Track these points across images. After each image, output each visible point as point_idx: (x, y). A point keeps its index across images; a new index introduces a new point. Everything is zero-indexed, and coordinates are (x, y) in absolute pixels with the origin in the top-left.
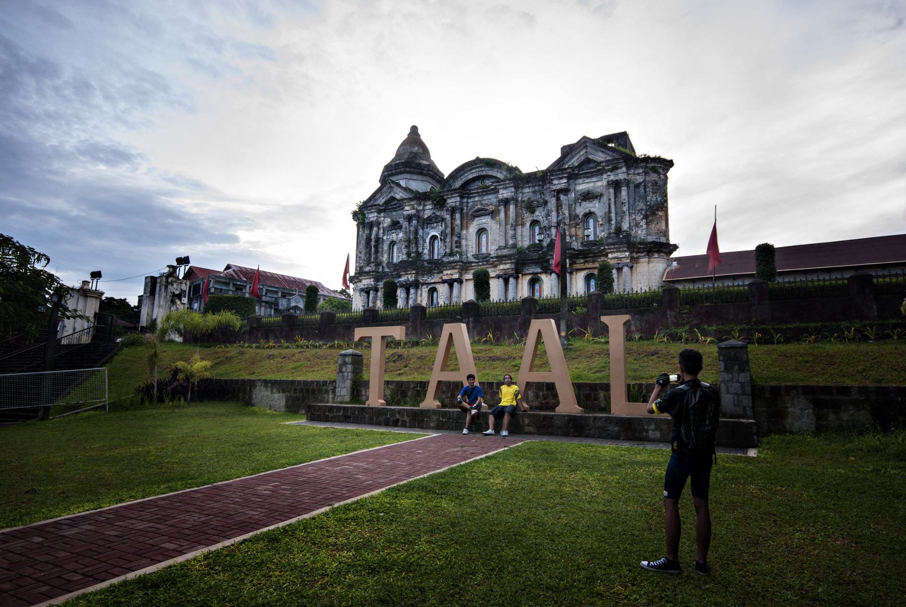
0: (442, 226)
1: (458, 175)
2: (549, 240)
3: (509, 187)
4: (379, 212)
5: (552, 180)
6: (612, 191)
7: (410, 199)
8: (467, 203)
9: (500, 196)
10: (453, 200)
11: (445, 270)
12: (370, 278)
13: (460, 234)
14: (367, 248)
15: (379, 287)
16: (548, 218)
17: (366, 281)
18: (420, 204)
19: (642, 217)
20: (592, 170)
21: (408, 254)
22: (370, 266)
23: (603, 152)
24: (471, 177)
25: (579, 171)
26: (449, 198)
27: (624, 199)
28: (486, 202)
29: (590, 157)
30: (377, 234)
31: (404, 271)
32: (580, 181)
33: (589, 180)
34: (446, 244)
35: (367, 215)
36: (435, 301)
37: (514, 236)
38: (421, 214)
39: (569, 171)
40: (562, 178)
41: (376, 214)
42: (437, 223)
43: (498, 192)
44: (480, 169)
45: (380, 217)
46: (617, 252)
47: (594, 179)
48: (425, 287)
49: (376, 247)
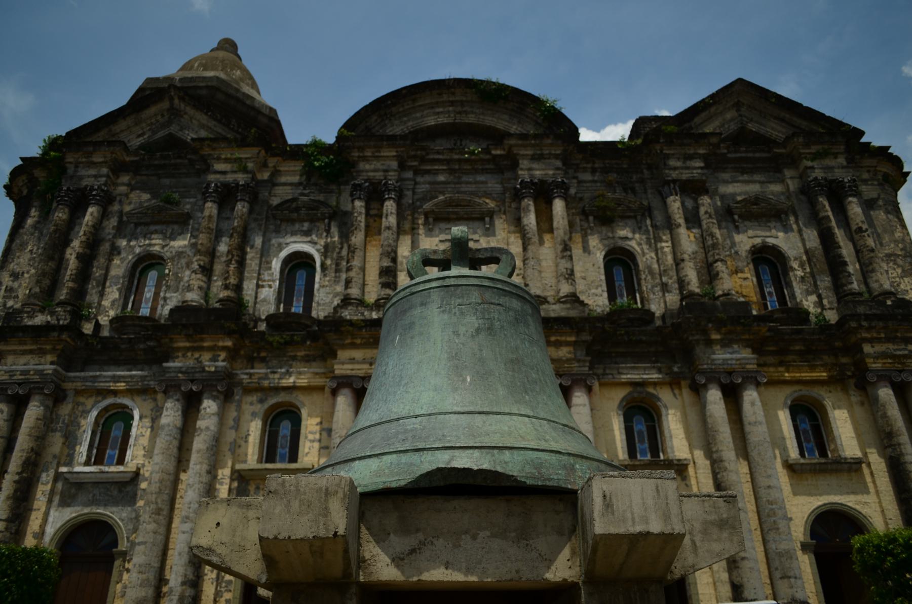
0: (328, 231)
1: (394, 109)
2: (673, 299)
3: (551, 156)
4: (118, 168)
5: (668, 157)
6: (823, 201)
7: (243, 143)
8: (416, 183)
9: (524, 175)
10: (378, 165)
11: (344, 347)
12: (42, 352)
13: (396, 252)
14: (51, 258)
15: (69, 386)
16: (659, 245)
17: (23, 359)
18: (265, 165)
19: (899, 271)
20: (758, 155)
21: (206, 293)
22: (52, 313)
23: (783, 120)
24: (431, 121)
25: (729, 152)
26: (365, 159)
27: (863, 222)
28: (472, 188)
29: (750, 126)
30: (97, 227)
31: (188, 337)
32: (726, 176)
33: (746, 177)
34: (352, 274)
35: (70, 171)
36: (283, 449)
37: (570, 275)
38: (264, 194)
39: (714, 140)
40: (691, 157)
41: (105, 170)
42: (312, 221)
43: (514, 166)
44: (459, 109)
45: (116, 185)
46: (888, 340)
47: (757, 177)
48: (254, 398)
49: (86, 260)
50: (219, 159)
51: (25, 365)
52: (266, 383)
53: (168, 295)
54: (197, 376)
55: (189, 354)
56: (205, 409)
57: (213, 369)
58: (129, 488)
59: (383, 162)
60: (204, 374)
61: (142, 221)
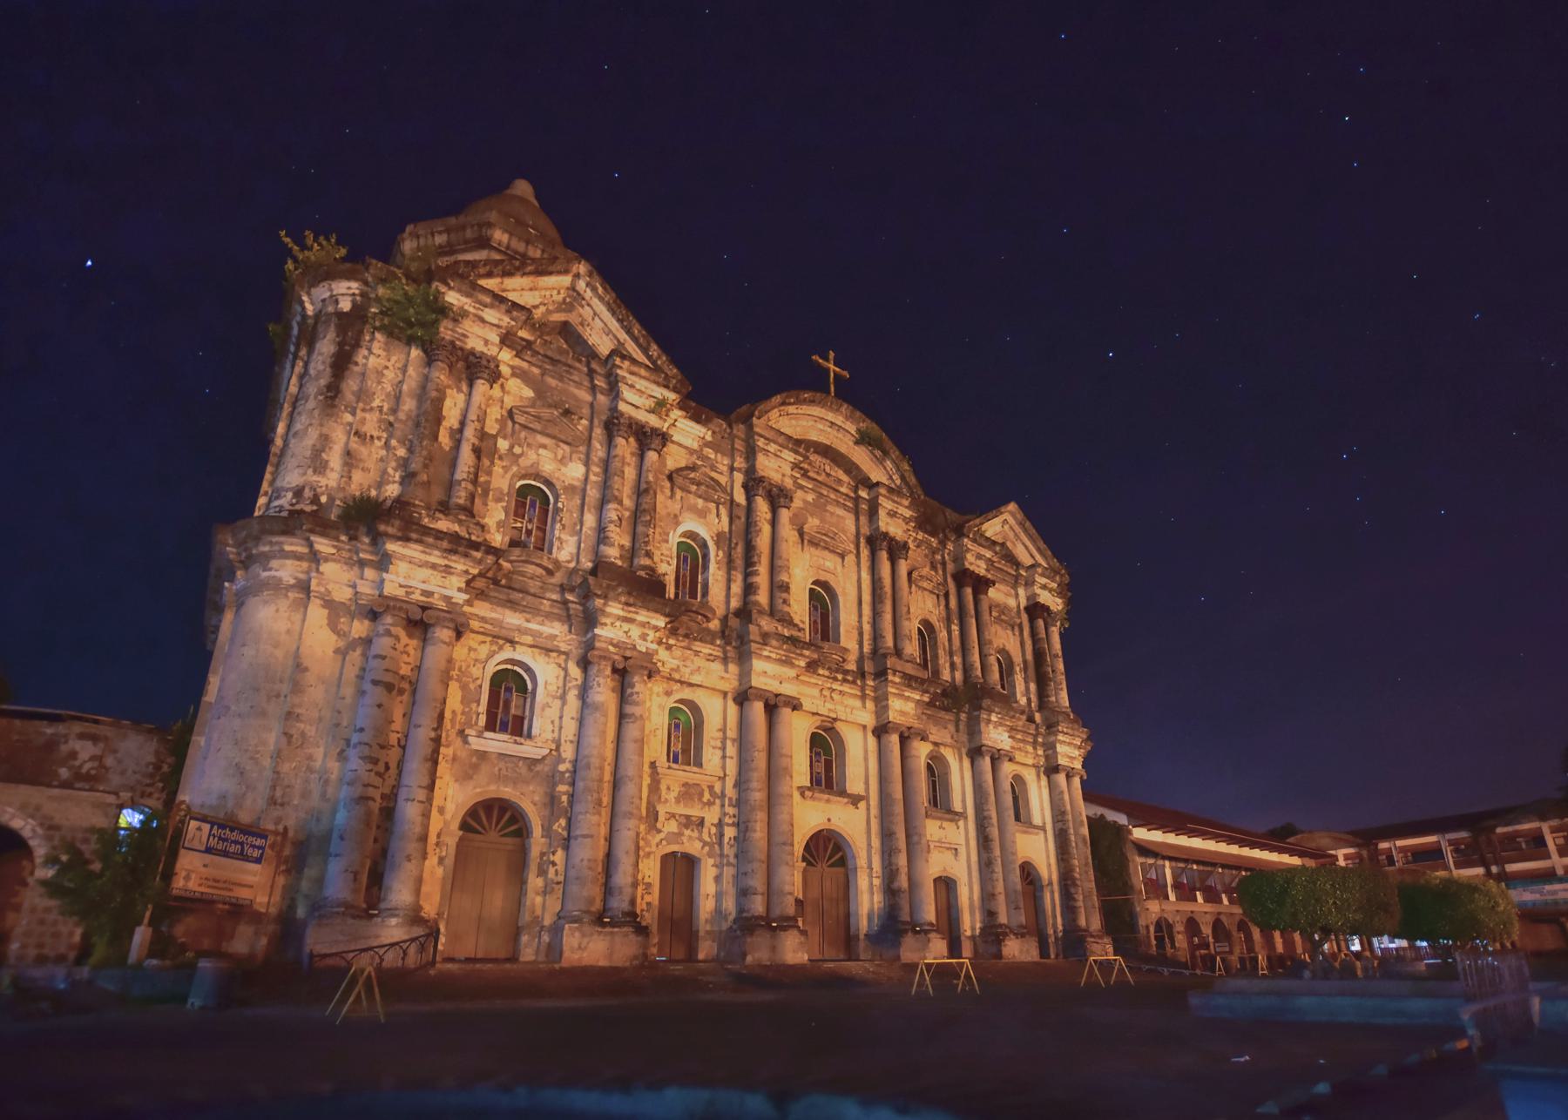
11: (760, 656)
50: (632, 386)
51: (424, 582)
52: (677, 676)
53: (563, 536)
54: (628, 654)
55: (618, 624)
56: (638, 693)
57: (644, 650)
58: (539, 768)
59: (779, 464)
60: (635, 653)
61: (531, 425)
